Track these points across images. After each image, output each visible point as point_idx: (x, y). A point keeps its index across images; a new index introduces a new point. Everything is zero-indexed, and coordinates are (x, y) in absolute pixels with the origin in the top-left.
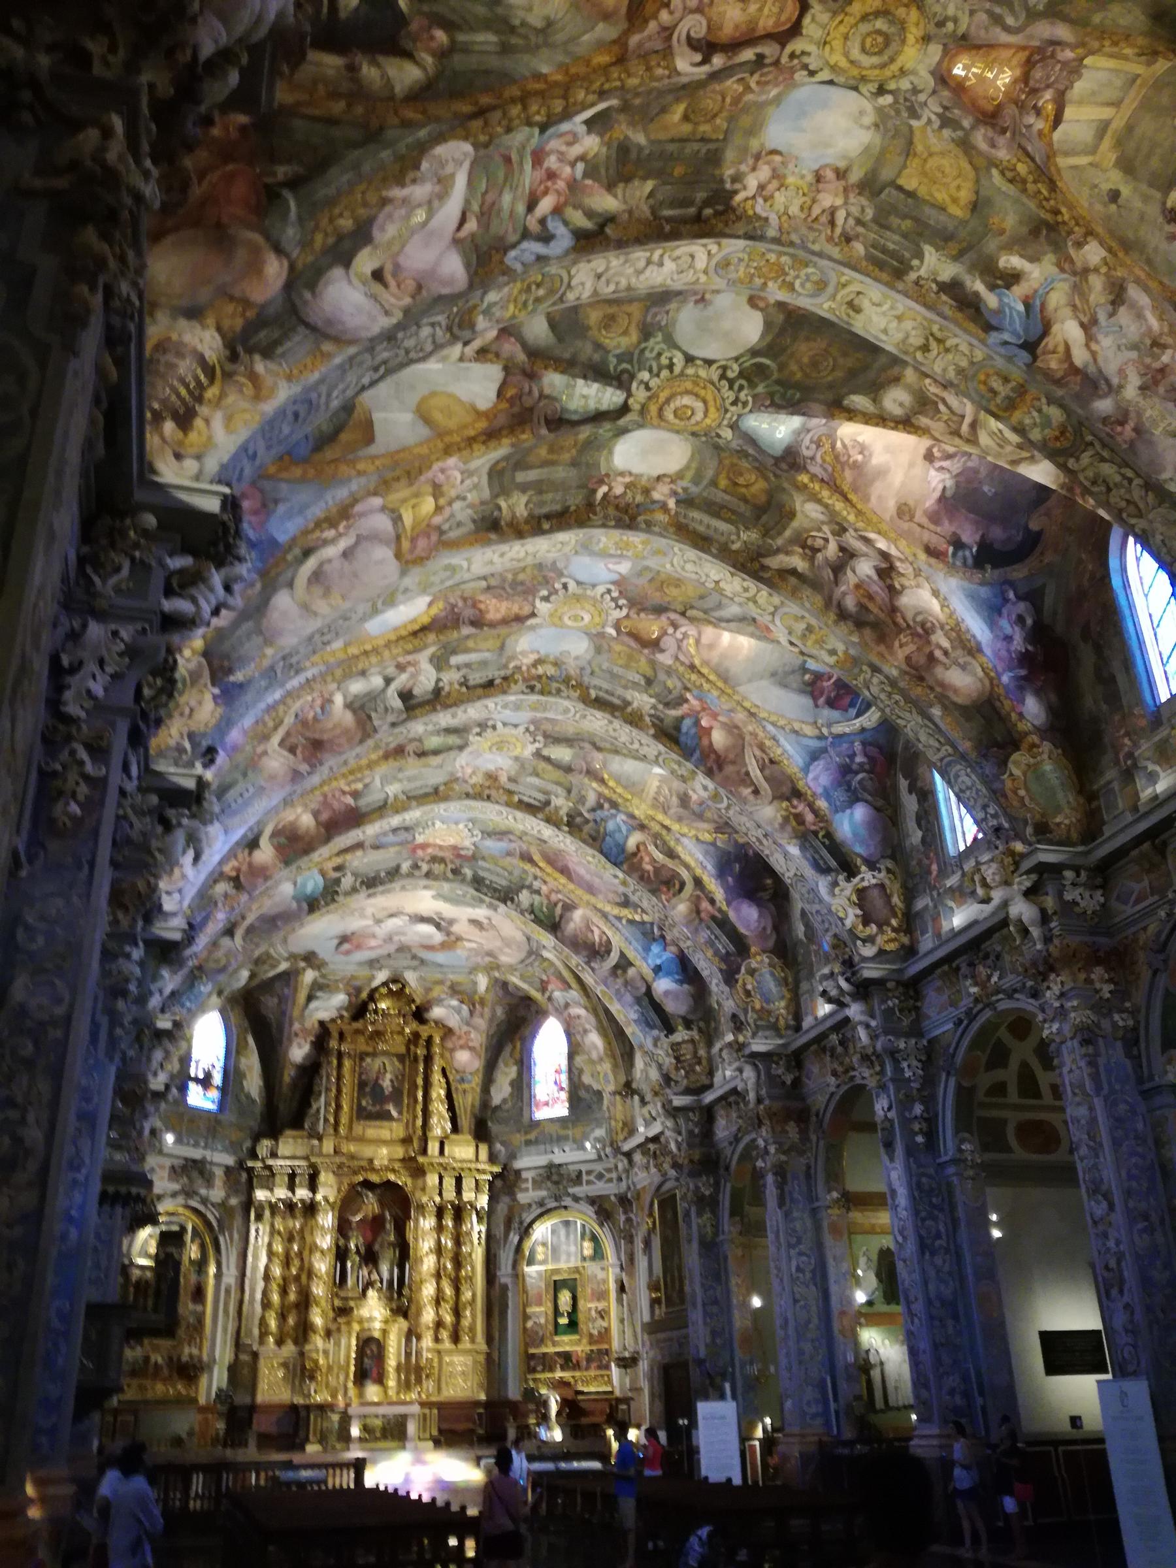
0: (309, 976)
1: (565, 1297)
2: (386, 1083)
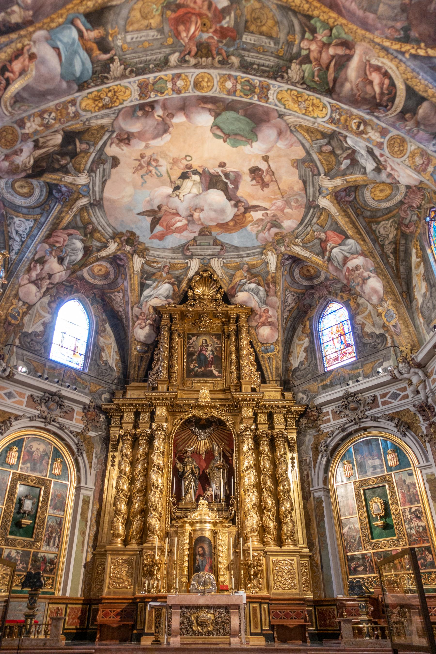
0: (137, 263)
1: (376, 506)
2: (208, 353)
